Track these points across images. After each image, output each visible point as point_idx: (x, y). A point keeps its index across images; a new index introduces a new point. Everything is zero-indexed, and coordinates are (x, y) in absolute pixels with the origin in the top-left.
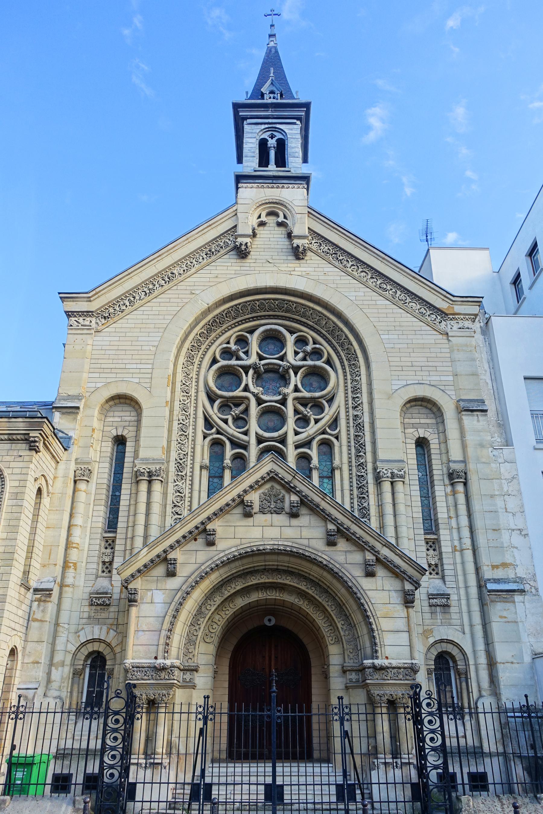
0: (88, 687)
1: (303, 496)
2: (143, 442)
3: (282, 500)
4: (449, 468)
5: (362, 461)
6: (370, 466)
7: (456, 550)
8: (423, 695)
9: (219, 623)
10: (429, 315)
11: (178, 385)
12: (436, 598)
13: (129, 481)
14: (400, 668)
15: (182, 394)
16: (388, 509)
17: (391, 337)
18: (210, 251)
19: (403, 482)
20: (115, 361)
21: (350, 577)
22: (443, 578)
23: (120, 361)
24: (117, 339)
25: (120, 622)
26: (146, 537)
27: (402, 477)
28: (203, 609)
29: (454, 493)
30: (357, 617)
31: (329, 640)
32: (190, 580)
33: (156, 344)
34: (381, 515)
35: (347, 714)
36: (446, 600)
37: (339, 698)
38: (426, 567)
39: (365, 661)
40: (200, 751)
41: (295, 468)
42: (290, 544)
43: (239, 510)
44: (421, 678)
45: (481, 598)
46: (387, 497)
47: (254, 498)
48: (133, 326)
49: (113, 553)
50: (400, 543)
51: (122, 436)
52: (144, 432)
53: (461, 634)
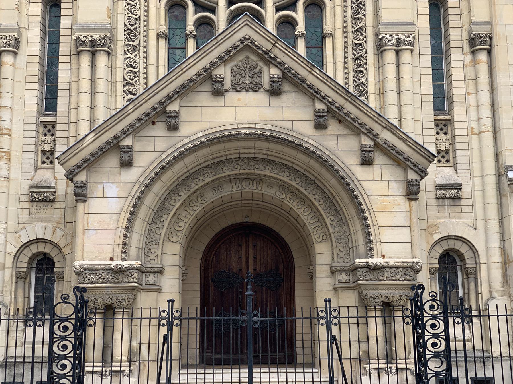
0: (36, 292)
1: (286, 69)
3: (260, 75)
4: (470, 32)
5: (360, 25)
6: (370, 33)
7: (472, 133)
8: (426, 297)
9: (186, 220)
12: (444, 189)
13: (68, 52)
14: (398, 267)
16: (391, 84)
19: (412, 51)
21: (342, 165)
22: (455, 166)
25: (68, 219)
26: (92, 121)
27: (411, 44)
28: (167, 204)
29: (475, 63)
30: (350, 212)
31: (315, 238)
32: (149, 171)
34: (382, 93)
35: (335, 318)
36: (456, 191)
37: (326, 301)
38: (435, 152)
39: (357, 261)
41: (276, 35)
42: (269, 127)
43: (207, 87)
44: (423, 277)
45: (499, 188)
46: (390, 70)
47: (224, 72)
49: (54, 141)
50: (403, 126)
53: (472, 229)
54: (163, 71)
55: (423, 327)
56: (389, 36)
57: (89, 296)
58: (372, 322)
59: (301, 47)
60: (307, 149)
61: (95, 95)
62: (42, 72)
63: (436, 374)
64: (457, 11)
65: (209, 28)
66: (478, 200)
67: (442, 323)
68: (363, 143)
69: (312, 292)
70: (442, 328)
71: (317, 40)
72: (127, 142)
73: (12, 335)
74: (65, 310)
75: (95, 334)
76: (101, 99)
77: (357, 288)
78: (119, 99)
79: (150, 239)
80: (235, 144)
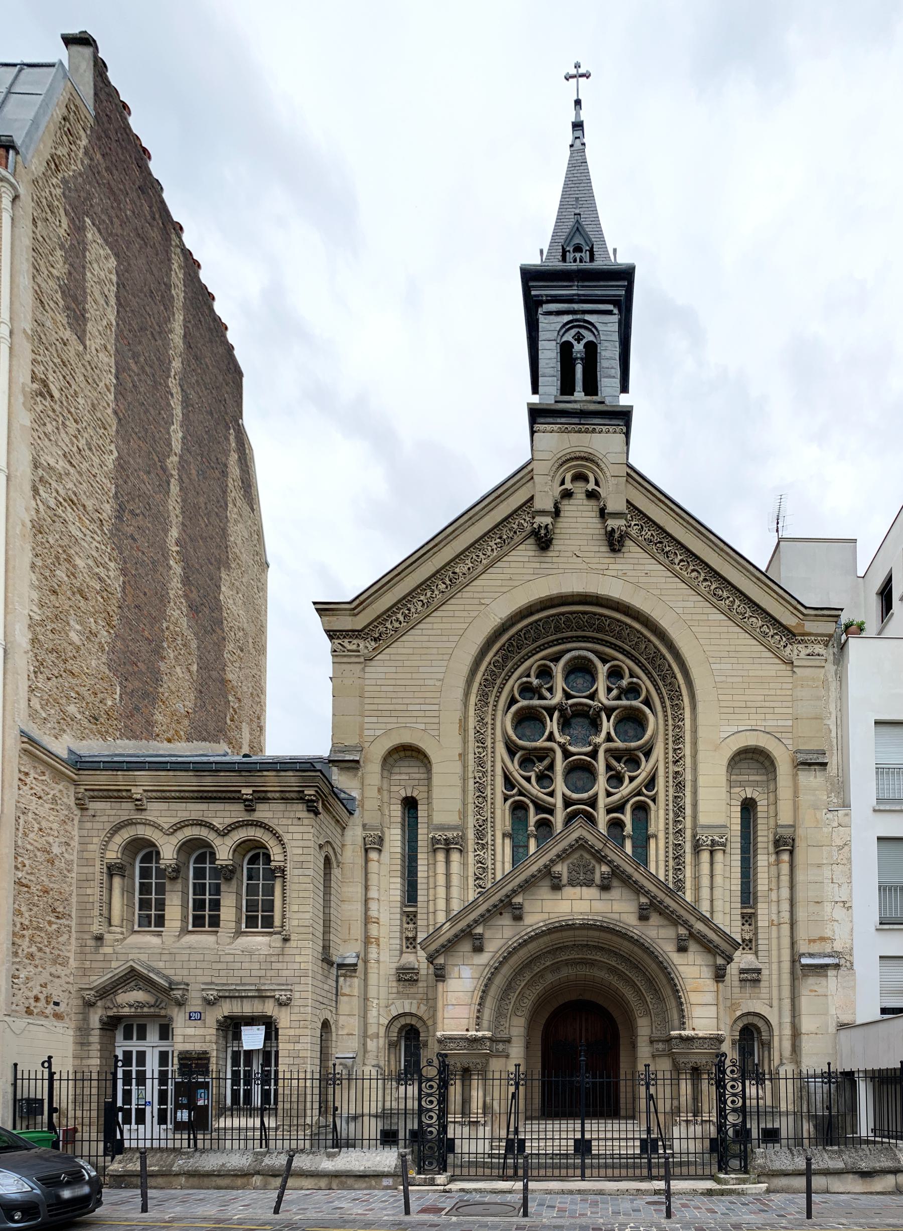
2: (436, 804)
4: (775, 834)
8: (728, 1062)
10: (772, 636)
11: (471, 732)
15: (477, 744)
16: (705, 881)
17: (723, 666)
18: (500, 538)
19: (724, 851)
20: (394, 701)
23: (400, 701)
24: (393, 670)
25: (430, 997)
26: (448, 911)
27: (724, 845)
28: (513, 984)
29: (778, 862)
31: (637, 1013)
33: (441, 676)
34: (697, 888)
35: (653, 1079)
37: (645, 1066)
38: (740, 941)
40: (513, 1111)
41: (606, 834)
44: (726, 1047)
45: (793, 973)
46: (705, 868)
48: (410, 651)
49: (416, 928)
50: (715, 918)
51: (412, 797)
52: (436, 792)
54: (508, 868)
55: (724, 1087)
56: (705, 837)
57: (450, 1061)
58: (683, 1084)
59: (628, 847)
60: (632, 937)
61: (450, 889)
62: (403, 867)
63: (734, 1125)
64: (765, 815)
65: (548, 829)
66: (775, 982)
67: (740, 1084)
68: (680, 932)
69: (634, 1059)
70: (740, 1088)
71: (642, 840)
72: (479, 930)
73: (388, 1091)
74: (431, 1072)
75: (455, 1091)
76: (455, 892)
77: (671, 1055)
78: (471, 892)
79: (499, 1014)
80: (571, 933)
